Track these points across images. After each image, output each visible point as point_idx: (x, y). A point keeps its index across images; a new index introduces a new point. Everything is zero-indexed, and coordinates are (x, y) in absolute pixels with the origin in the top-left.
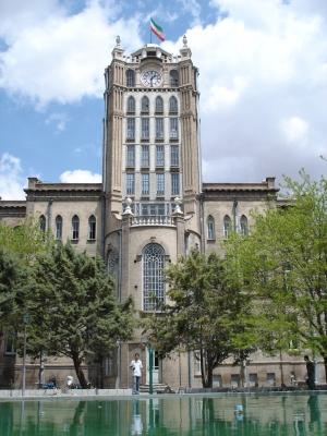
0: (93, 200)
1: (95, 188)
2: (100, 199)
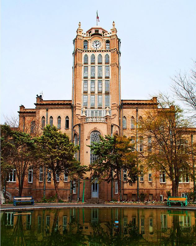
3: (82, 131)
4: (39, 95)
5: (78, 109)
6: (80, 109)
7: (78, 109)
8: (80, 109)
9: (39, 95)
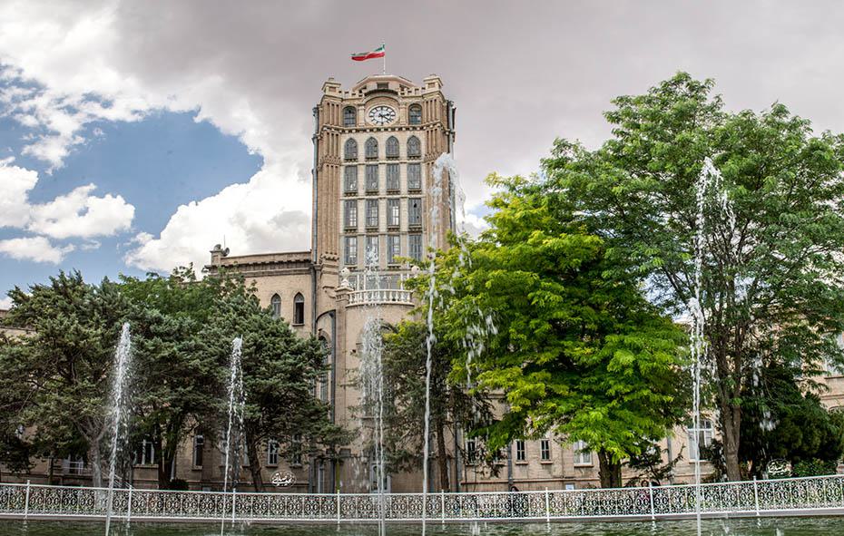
0: (300, 273)
1: (301, 258)
2: (308, 272)
3: (340, 328)
4: (223, 248)
5: (330, 273)
6: (335, 273)
7: (330, 273)
8: (335, 273)
9: (223, 248)
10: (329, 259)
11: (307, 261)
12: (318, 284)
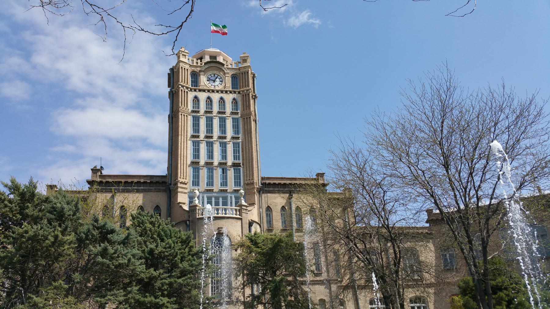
0: (159, 191)
1: (161, 180)
2: (164, 191)
5: (182, 192)
6: (185, 193)
7: (182, 192)
8: (185, 193)
10: (181, 183)
11: (164, 183)
12: (172, 200)
